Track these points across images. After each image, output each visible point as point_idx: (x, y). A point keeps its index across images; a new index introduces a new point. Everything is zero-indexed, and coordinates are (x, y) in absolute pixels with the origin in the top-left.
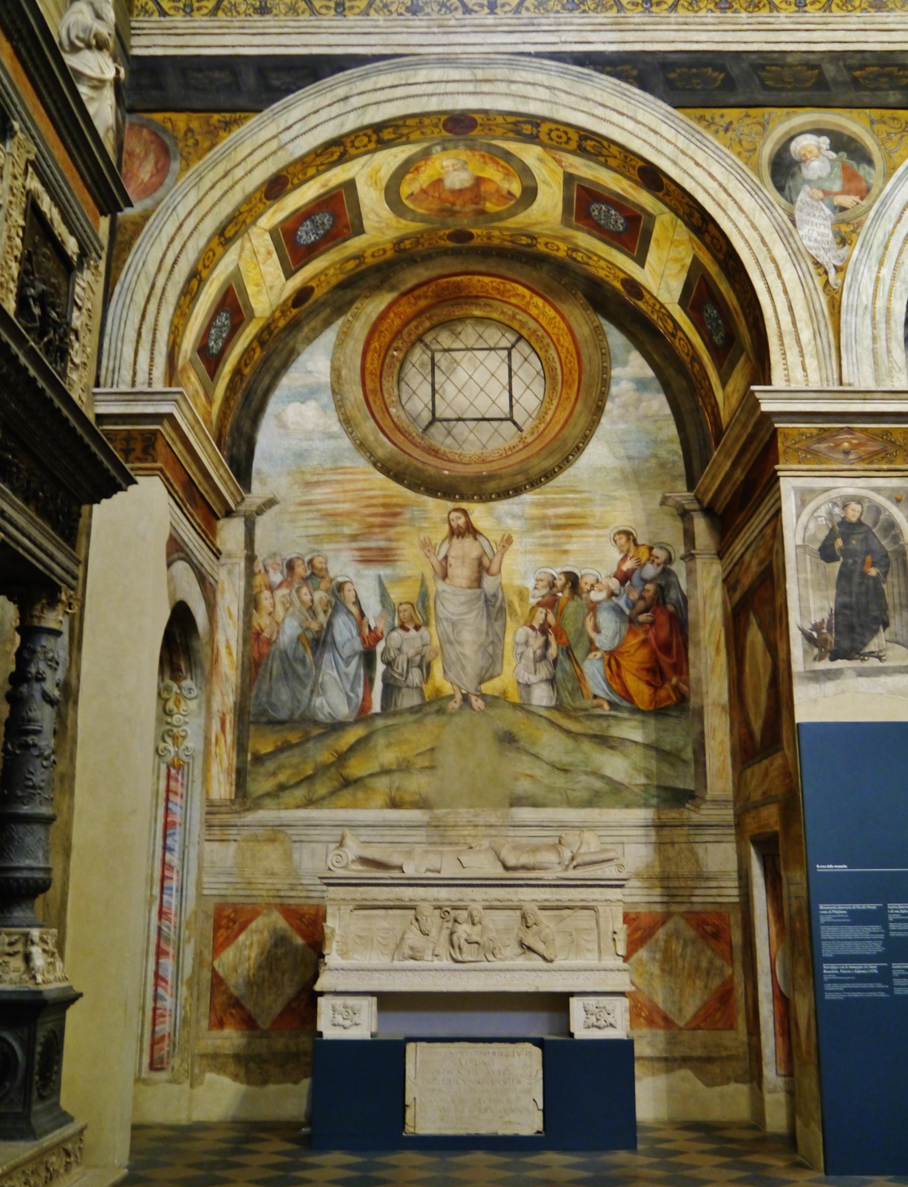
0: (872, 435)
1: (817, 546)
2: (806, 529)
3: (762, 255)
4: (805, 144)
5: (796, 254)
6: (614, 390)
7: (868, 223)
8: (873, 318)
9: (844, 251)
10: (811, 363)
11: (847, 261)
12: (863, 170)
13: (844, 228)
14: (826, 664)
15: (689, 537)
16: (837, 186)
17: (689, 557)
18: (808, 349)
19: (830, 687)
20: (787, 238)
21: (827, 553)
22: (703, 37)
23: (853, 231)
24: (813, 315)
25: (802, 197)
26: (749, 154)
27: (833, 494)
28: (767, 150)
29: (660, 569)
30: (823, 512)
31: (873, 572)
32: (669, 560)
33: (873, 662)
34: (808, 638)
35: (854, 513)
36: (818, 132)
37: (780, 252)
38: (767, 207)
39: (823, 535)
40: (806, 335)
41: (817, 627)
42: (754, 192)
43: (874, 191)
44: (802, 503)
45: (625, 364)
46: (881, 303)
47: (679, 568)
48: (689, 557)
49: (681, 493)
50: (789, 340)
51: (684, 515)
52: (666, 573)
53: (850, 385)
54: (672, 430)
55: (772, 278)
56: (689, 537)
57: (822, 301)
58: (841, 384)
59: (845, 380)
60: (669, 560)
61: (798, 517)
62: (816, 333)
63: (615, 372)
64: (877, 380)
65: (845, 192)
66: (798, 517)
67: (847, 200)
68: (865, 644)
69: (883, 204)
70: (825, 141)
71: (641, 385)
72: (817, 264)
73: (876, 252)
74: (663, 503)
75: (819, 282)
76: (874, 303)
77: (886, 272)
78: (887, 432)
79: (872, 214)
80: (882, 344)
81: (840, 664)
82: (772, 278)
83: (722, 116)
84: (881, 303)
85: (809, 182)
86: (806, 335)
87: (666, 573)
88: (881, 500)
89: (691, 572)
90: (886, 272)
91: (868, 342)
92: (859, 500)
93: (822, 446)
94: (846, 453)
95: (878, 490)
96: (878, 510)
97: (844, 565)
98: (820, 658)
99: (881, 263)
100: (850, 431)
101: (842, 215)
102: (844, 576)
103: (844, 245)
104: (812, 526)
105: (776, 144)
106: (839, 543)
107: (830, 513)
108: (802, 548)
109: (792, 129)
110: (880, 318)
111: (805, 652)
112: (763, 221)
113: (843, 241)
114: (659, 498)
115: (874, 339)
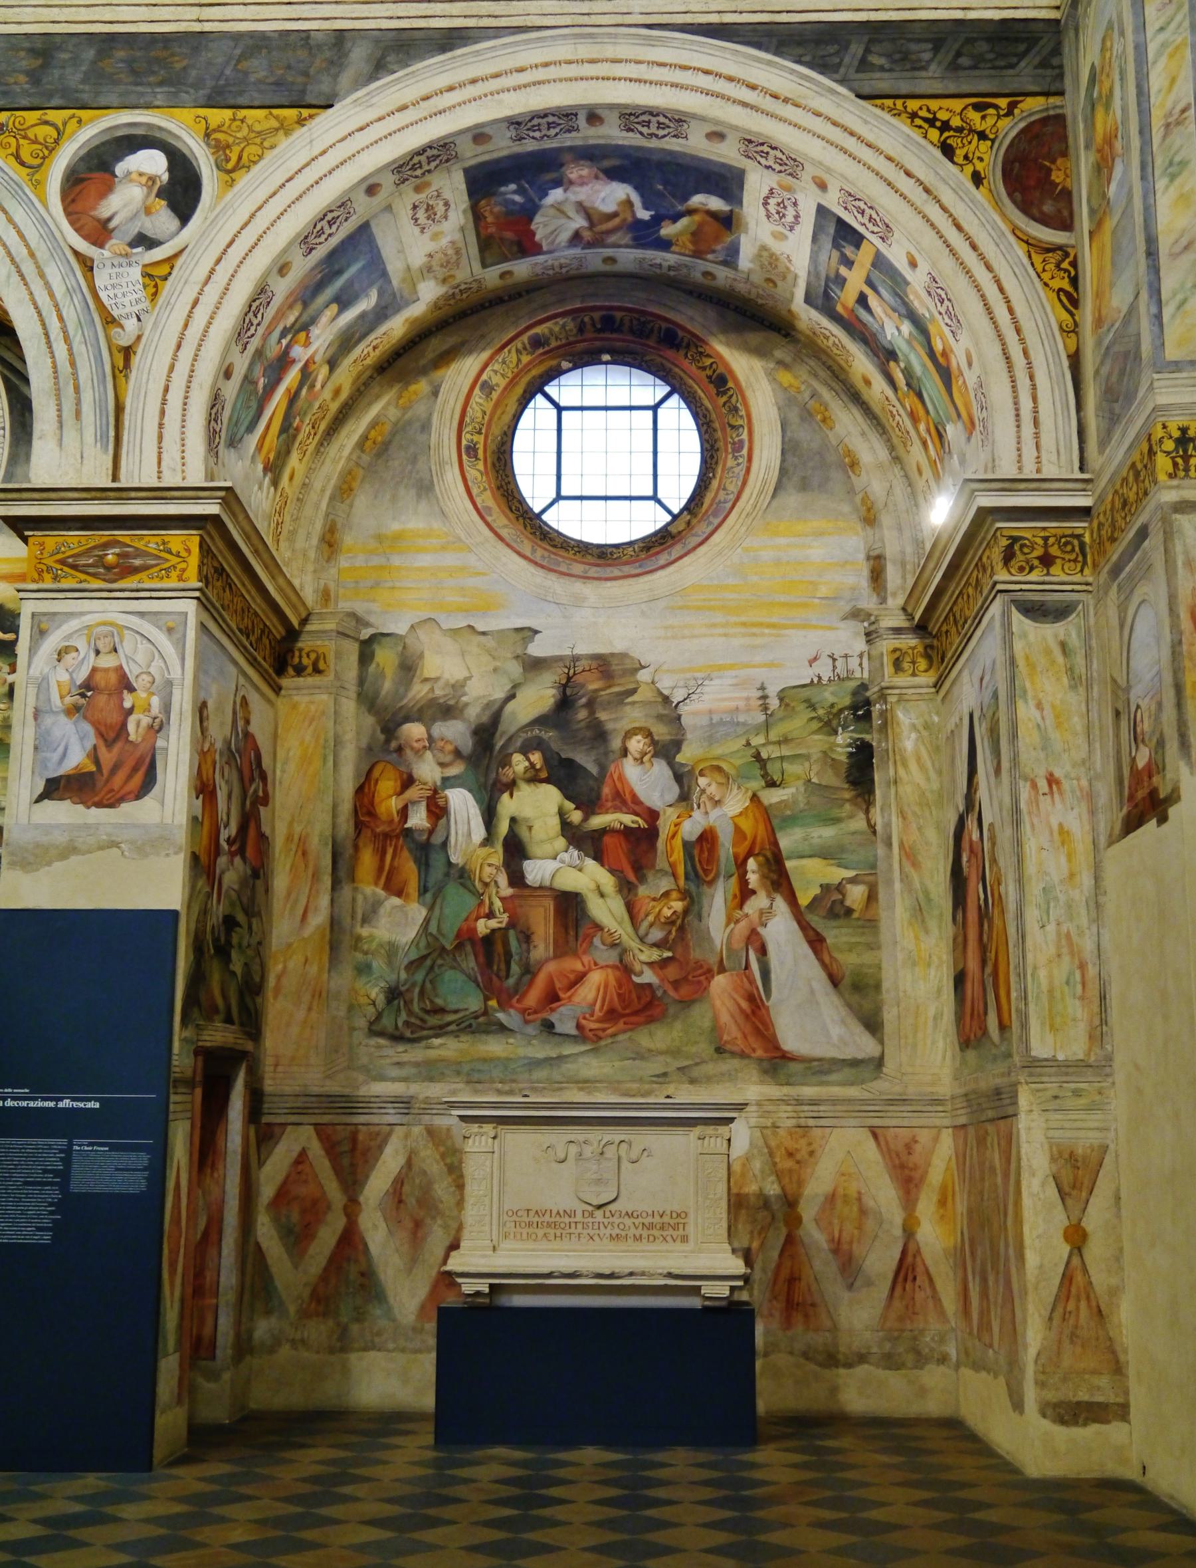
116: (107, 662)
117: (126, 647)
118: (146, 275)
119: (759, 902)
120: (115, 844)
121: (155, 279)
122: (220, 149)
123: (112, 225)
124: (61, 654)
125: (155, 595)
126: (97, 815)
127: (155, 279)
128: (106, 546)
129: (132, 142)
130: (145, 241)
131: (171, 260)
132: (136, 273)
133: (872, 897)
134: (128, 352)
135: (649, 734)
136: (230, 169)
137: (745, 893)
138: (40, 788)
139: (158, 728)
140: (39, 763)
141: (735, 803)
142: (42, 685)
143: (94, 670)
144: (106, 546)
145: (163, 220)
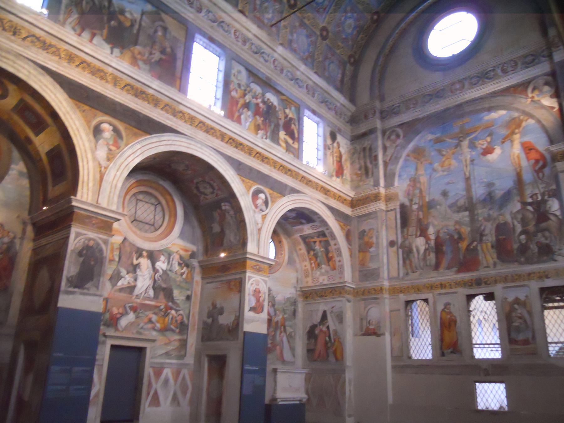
0: (102, 221)
1: (77, 251)
2: (76, 245)
3: (84, 155)
4: (105, 126)
5: (95, 159)
6: (10, 172)
7: (117, 157)
8: (111, 186)
9: (108, 163)
10: (90, 194)
11: (109, 166)
12: (119, 141)
13: (110, 156)
14: (71, 289)
15: (24, 232)
16: (111, 143)
17: (22, 238)
18: (91, 189)
19: (71, 296)
20: (93, 153)
21: (80, 254)
22: (84, 80)
23: (113, 158)
24: (94, 179)
25: (101, 142)
26: (88, 122)
27: (87, 236)
28: (94, 123)
29: (10, 240)
30: (82, 241)
31: (92, 263)
32: (14, 238)
33: (86, 291)
34: (68, 280)
35: (91, 243)
36: (110, 124)
37: (90, 156)
38: (89, 141)
39: (80, 248)
40: (91, 184)
41: (71, 277)
42: (87, 135)
43: (121, 148)
44: (76, 237)
45: (17, 164)
46: (115, 182)
47: (17, 241)
48: (22, 238)
49: (25, 215)
50: (85, 184)
51: (24, 223)
52: (12, 242)
53: (100, 204)
54: (28, 193)
55: (85, 163)
56: (24, 232)
57: (98, 176)
58: (97, 203)
59: (99, 202)
60: (14, 238)
61: (74, 240)
62: (94, 185)
63: (13, 166)
64: (108, 205)
65: (113, 145)
66: (74, 240)
67: (113, 148)
68: (85, 285)
69: (123, 153)
70: (111, 128)
71: (21, 174)
72: (100, 164)
73: (117, 167)
74: (18, 217)
75: (98, 170)
76: (113, 182)
77: (118, 173)
78: (107, 221)
79: (119, 155)
80: (112, 195)
81: (76, 290)
82: (85, 163)
83: (83, 107)
84: (115, 182)
85: (104, 138)
86: (91, 184)
87: (12, 242)
88: (100, 242)
89: (21, 244)
90: (118, 173)
91: (108, 193)
92: (94, 240)
93: (87, 221)
94: (94, 224)
95: (100, 238)
96: (98, 244)
97: (84, 259)
98: (70, 287)
99: (118, 170)
100: (96, 218)
101: (110, 152)
102: (84, 262)
103: (108, 161)
104: (78, 244)
105: (97, 122)
106: (84, 252)
107: (84, 242)
108: (73, 251)
109: (102, 120)
110: (114, 186)
111: (66, 285)
112: (87, 145)
113: (109, 159)
114: (16, 215)
115: (110, 192)
116: (258, 287)
117: (260, 285)
118: (262, 217)
119: (283, 334)
120: (258, 321)
121: (264, 217)
122: (271, 197)
123: (258, 205)
124: (252, 284)
125: (264, 276)
126: (256, 315)
127: (264, 217)
128: (257, 265)
129: (262, 192)
130: (262, 211)
131: (266, 215)
132: (260, 216)
133: (295, 334)
134: (260, 230)
135: (272, 302)
136: (273, 202)
137: (281, 332)
138: (249, 309)
139: (264, 300)
140: (249, 304)
141: (281, 317)
142: (249, 289)
143: (256, 288)
144: (257, 265)
145: (264, 207)
